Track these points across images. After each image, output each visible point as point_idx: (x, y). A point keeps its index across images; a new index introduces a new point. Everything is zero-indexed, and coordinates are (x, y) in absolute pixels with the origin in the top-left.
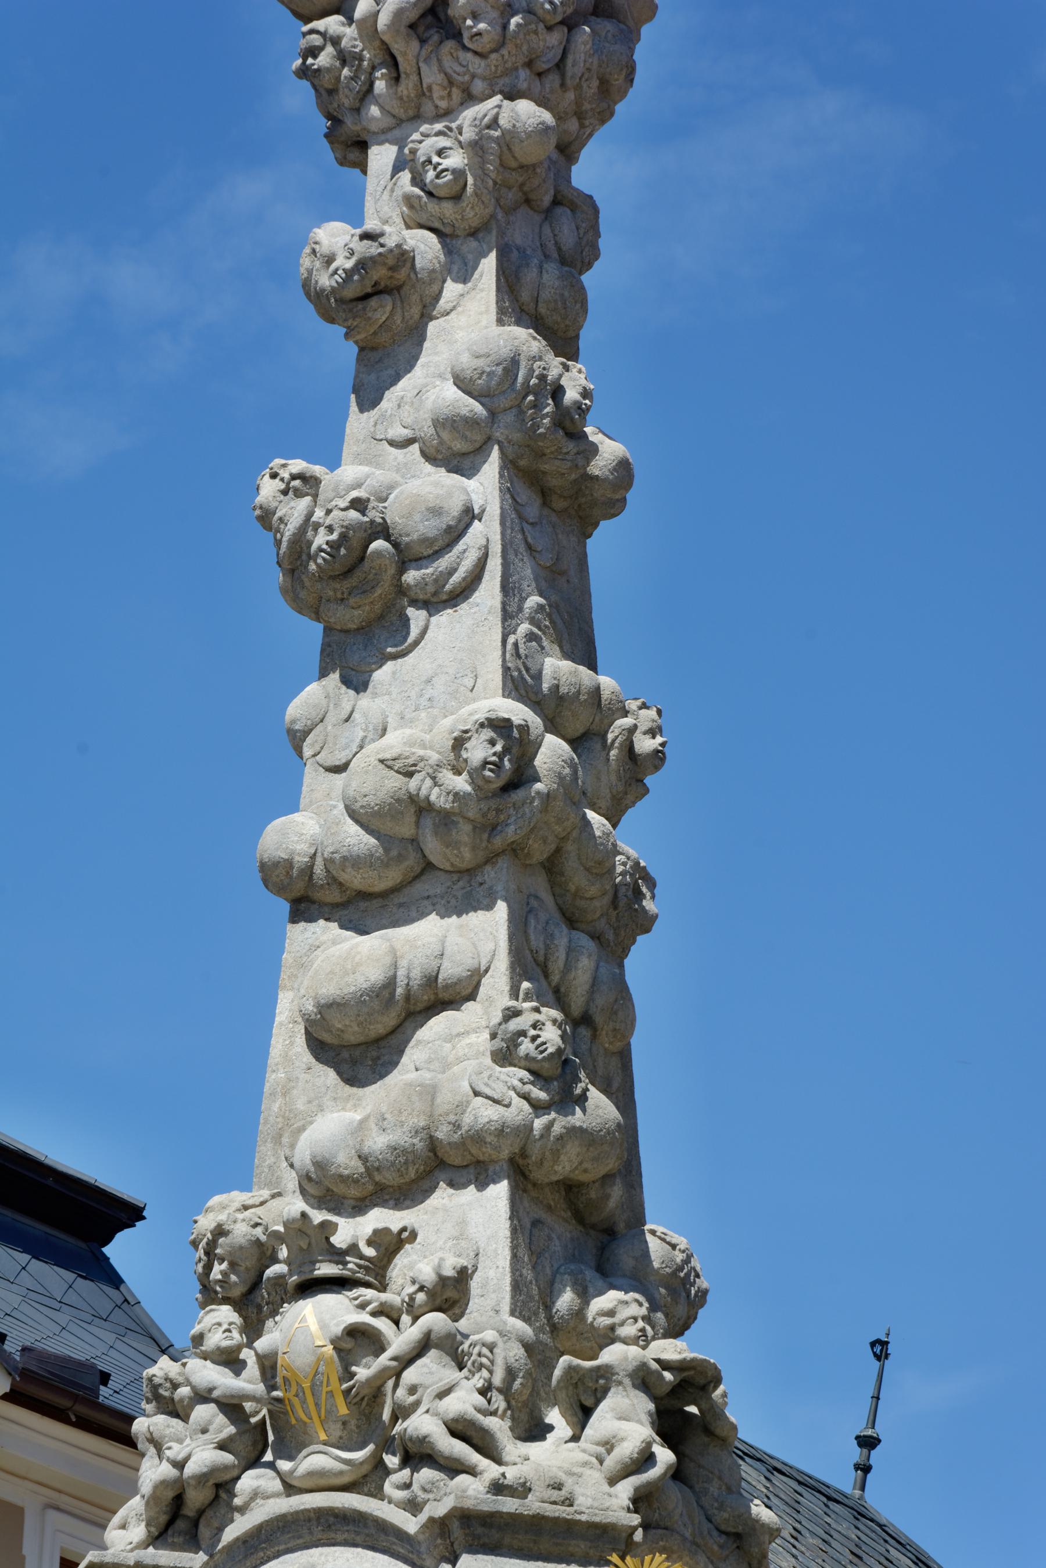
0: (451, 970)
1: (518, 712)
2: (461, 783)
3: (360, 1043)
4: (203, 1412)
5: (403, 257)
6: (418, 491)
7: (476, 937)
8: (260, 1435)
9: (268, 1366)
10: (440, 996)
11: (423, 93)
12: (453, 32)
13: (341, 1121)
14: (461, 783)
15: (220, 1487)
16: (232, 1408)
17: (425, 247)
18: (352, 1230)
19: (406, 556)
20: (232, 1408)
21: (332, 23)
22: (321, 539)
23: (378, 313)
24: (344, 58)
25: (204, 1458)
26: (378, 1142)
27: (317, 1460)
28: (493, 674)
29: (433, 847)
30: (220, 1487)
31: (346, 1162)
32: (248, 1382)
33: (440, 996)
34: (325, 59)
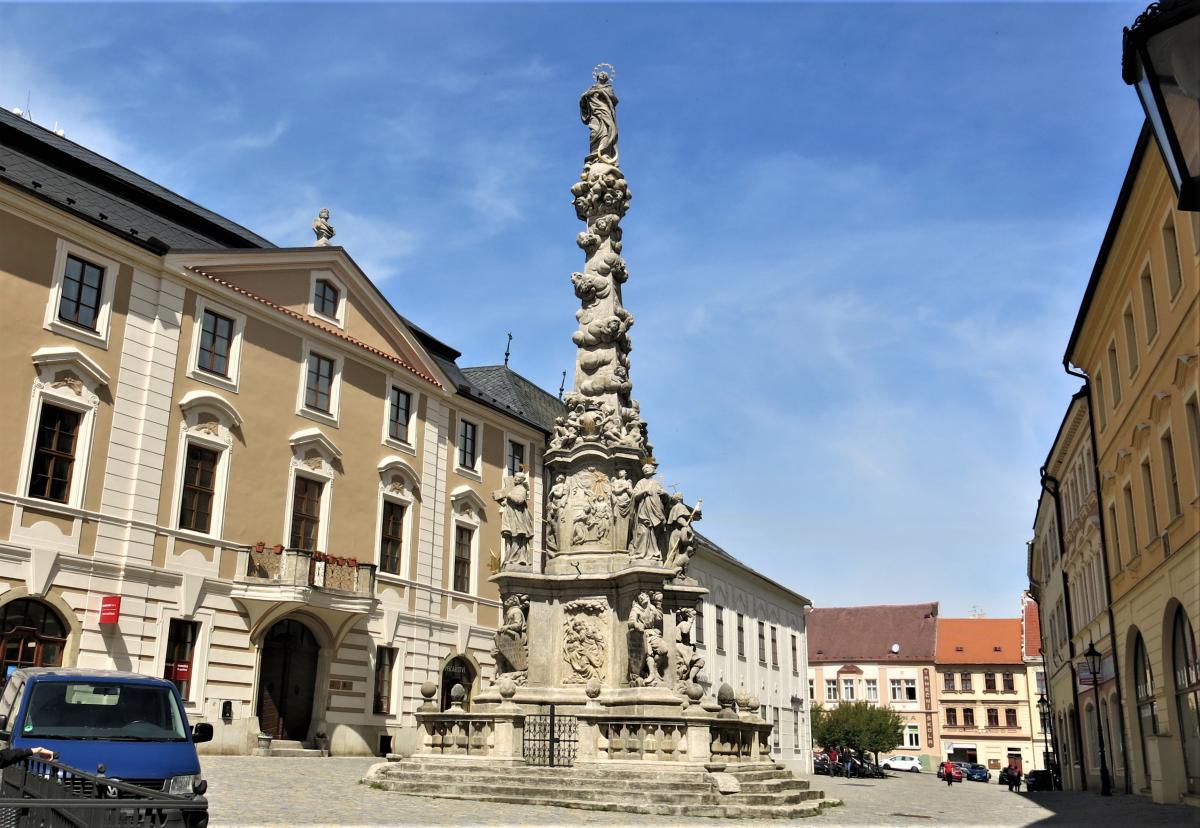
0: (607, 359)
1: (617, 319)
2: (609, 330)
3: (590, 369)
4: (571, 428)
5: (595, 240)
6: (599, 279)
7: (610, 354)
8: (581, 432)
9: (581, 422)
10: (604, 363)
11: (597, 211)
12: (604, 202)
13: (588, 382)
14: (609, 330)
15: (574, 440)
16: (576, 428)
17: (598, 237)
18: (596, 399)
19: (598, 290)
20: (576, 428)
21: (582, 198)
22: (583, 287)
23: (590, 248)
24: (585, 204)
25: (572, 436)
26: (595, 386)
27: (590, 437)
28: (612, 311)
29: (603, 339)
30: (574, 440)
31: (590, 389)
32: (577, 423)
33: (604, 363)
34: (581, 204)
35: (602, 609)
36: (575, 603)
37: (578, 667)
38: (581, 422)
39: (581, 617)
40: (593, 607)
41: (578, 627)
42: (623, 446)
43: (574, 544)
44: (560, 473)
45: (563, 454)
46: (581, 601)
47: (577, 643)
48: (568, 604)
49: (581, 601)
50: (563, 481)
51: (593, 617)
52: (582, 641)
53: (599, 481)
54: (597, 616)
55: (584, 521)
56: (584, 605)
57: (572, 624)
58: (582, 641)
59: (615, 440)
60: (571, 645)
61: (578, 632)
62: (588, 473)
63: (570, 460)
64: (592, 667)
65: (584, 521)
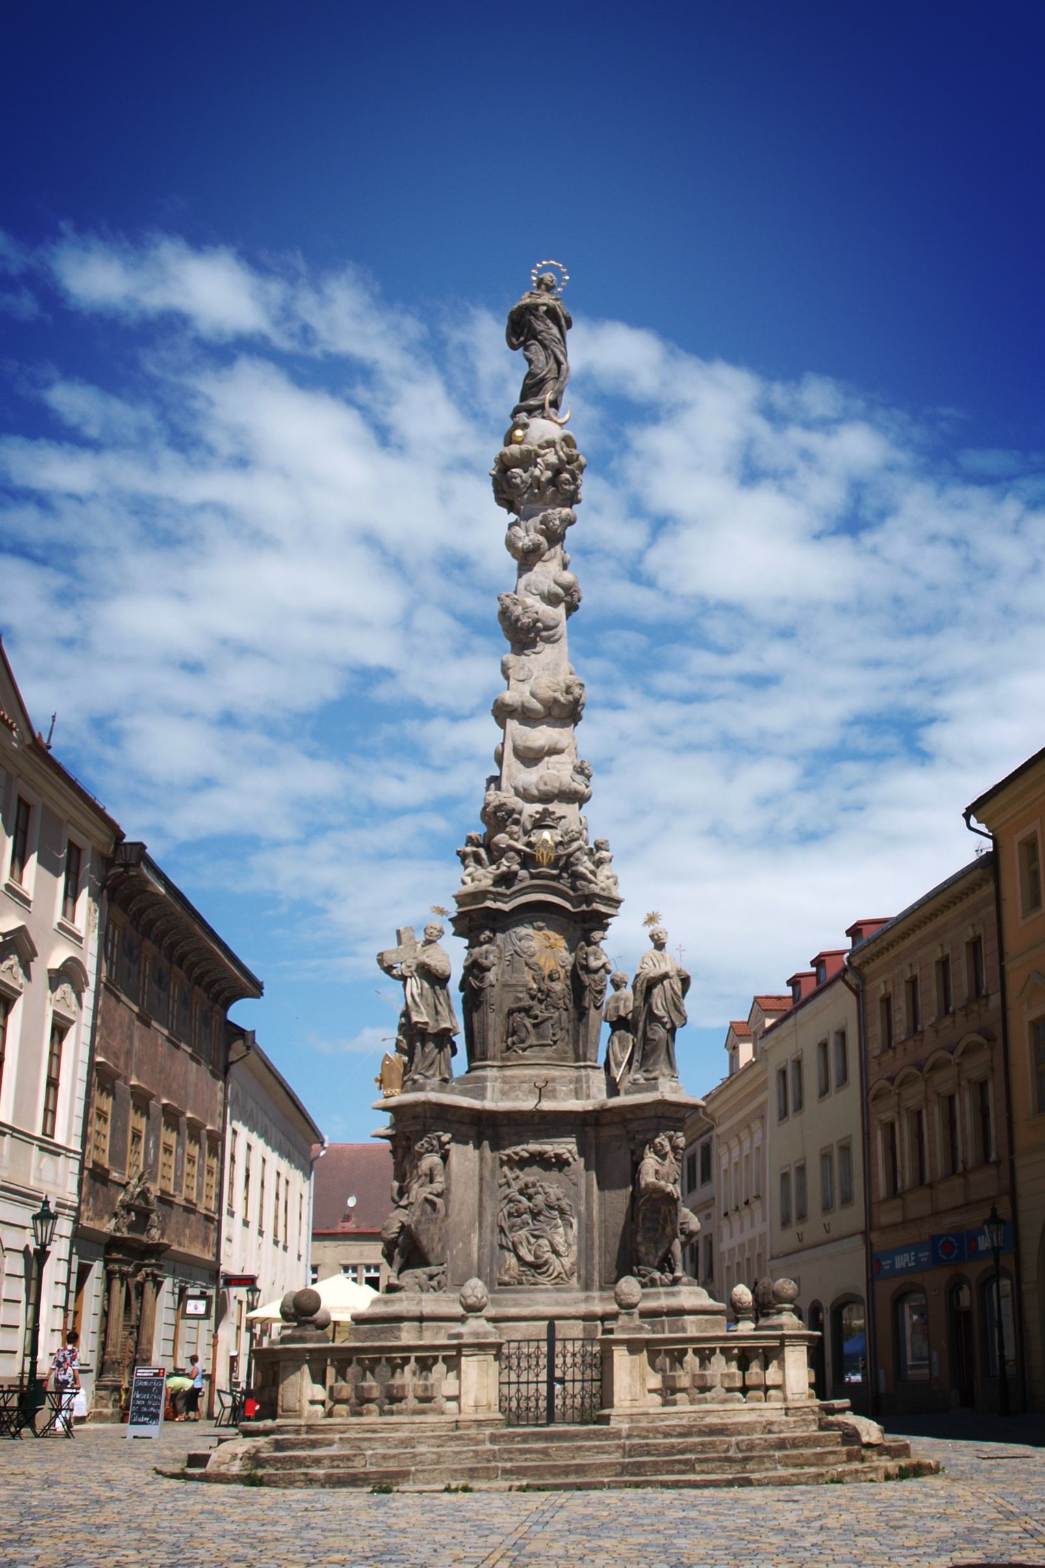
35: (571, 1160)
36: (524, 1149)
37: (530, 1258)
38: (529, 844)
39: (532, 1174)
40: (557, 1156)
41: (531, 1191)
42: (602, 893)
43: (508, 1048)
44: (486, 928)
45: (497, 897)
46: (534, 1147)
47: (527, 1217)
48: (508, 1151)
49: (534, 1147)
50: (490, 941)
51: (554, 1173)
52: (535, 1215)
53: (551, 947)
54: (560, 1171)
55: (527, 1010)
56: (541, 1154)
57: (516, 1186)
58: (535, 1215)
59: (590, 882)
60: (519, 1220)
61: (530, 1198)
62: (530, 931)
63: (506, 907)
64: (554, 1256)
65: (527, 1010)
